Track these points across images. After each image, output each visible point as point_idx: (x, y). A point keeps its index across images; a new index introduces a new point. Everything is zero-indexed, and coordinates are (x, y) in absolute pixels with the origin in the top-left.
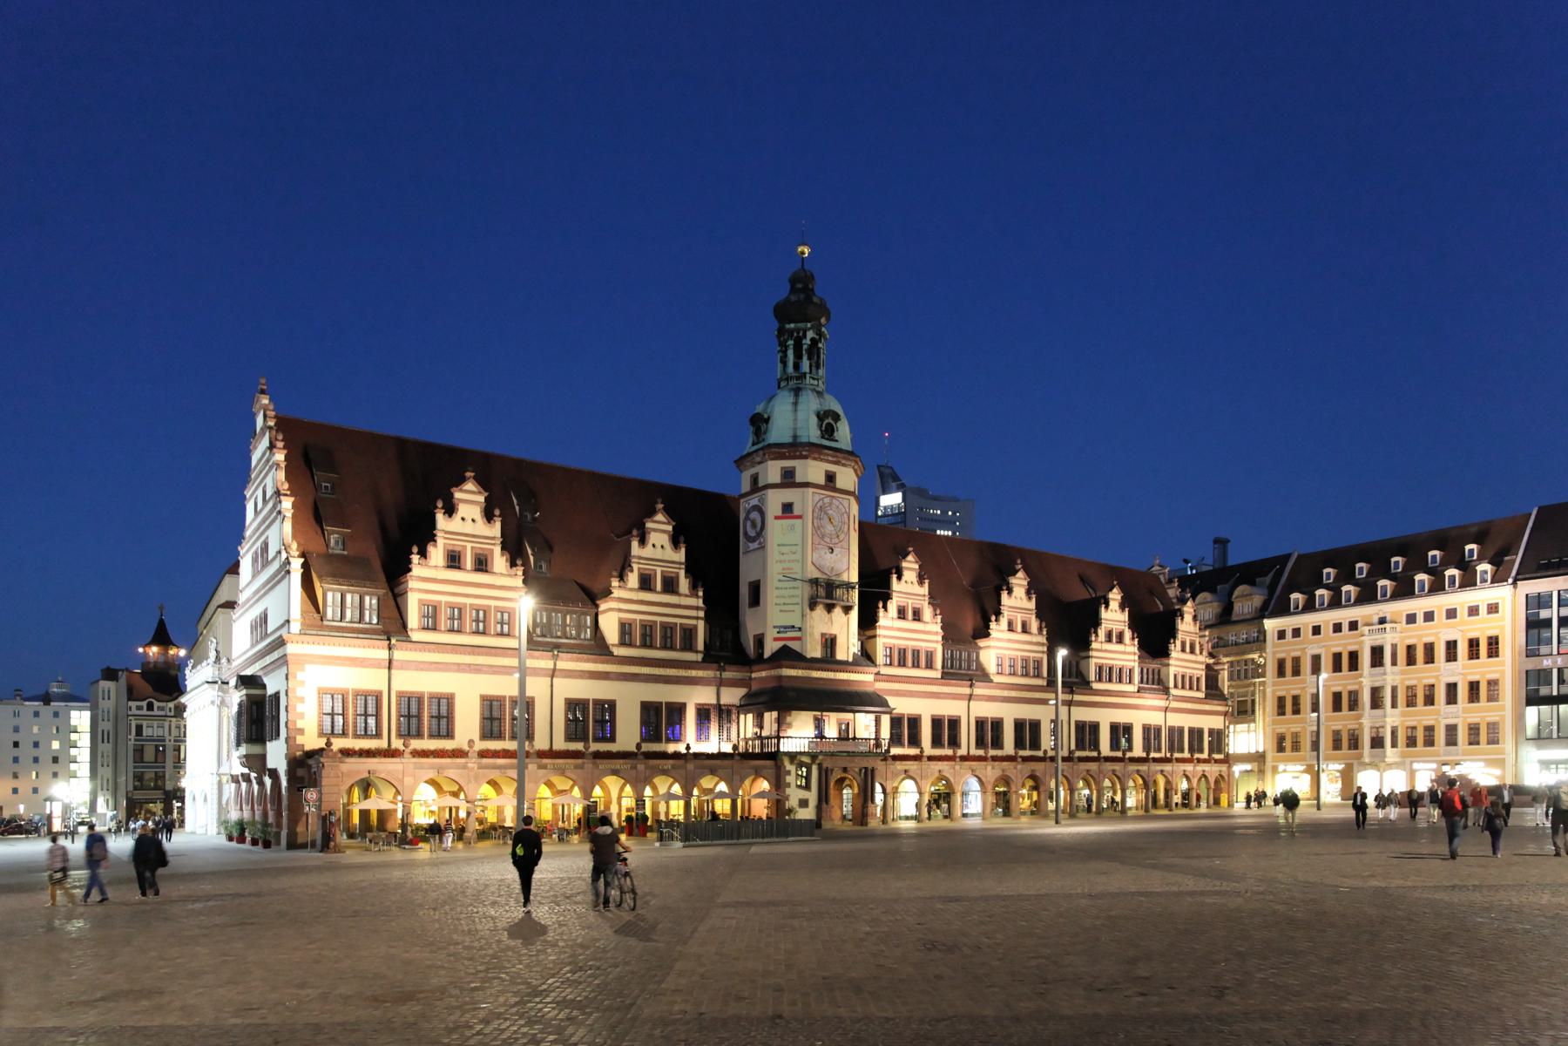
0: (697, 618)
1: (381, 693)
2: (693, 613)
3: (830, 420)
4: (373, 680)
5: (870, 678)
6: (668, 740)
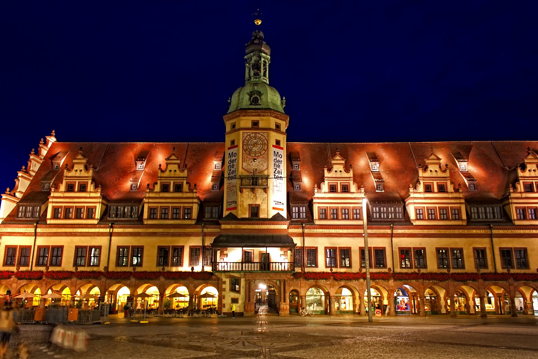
0: (193, 203)
1: (31, 246)
2: (191, 200)
3: (256, 96)
4: (27, 241)
5: (285, 227)
6: (173, 265)
